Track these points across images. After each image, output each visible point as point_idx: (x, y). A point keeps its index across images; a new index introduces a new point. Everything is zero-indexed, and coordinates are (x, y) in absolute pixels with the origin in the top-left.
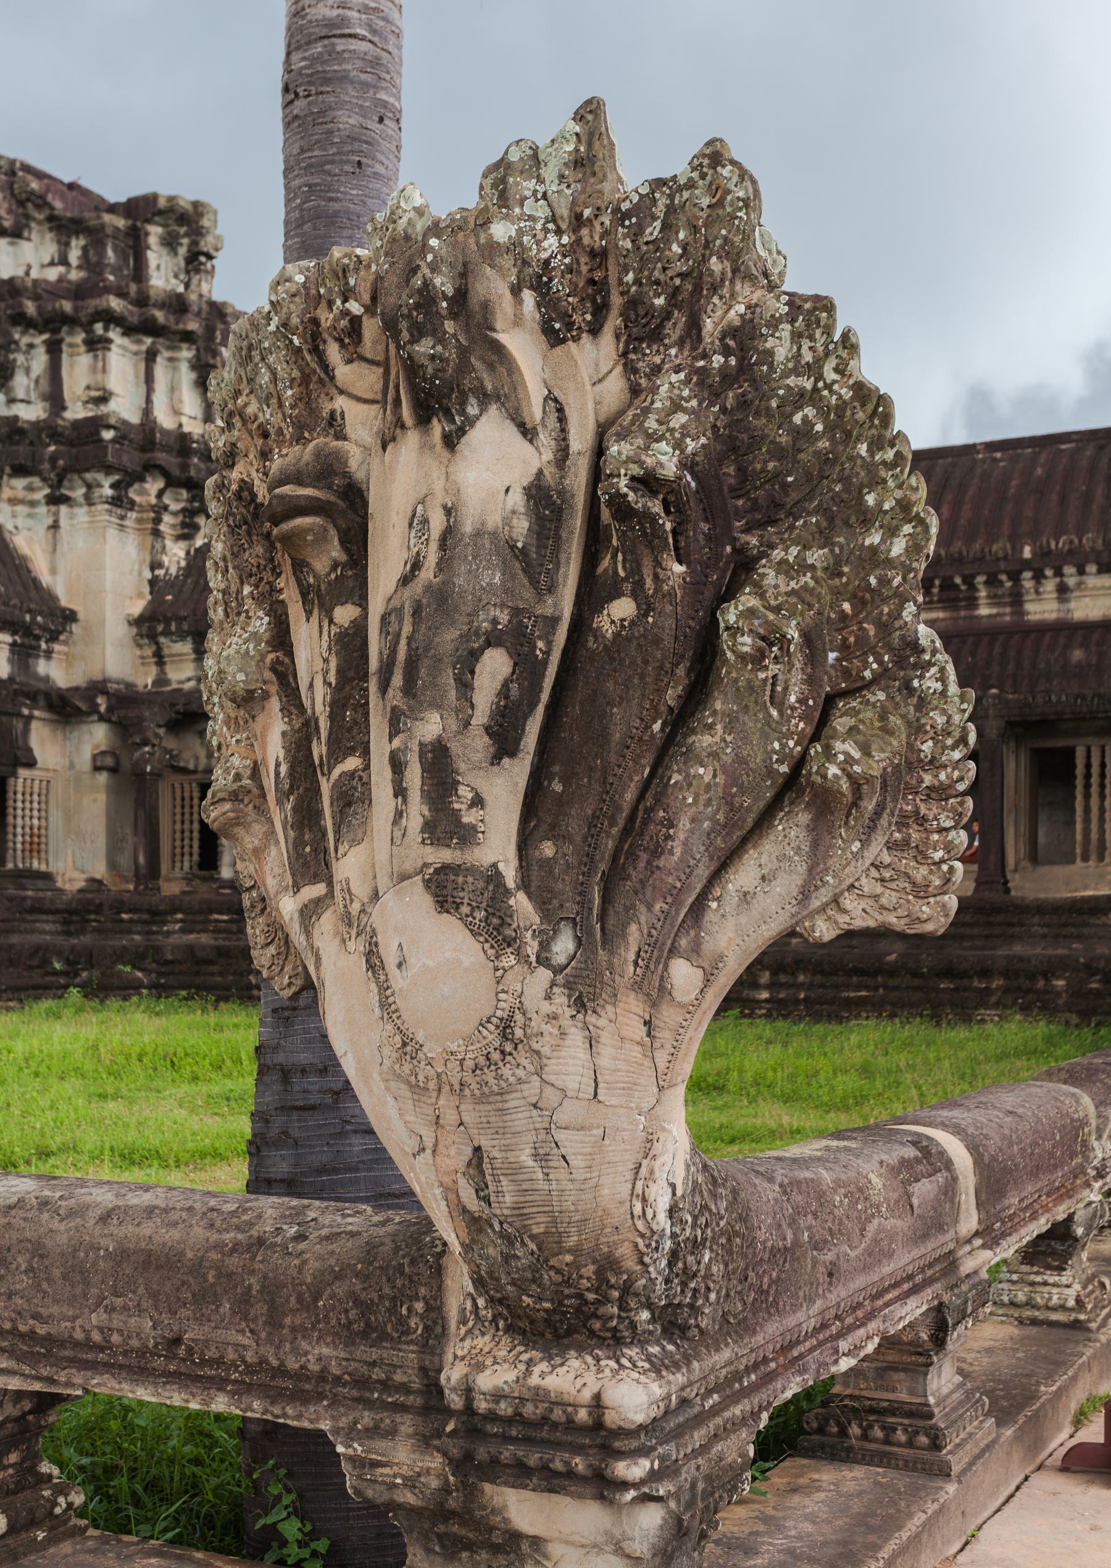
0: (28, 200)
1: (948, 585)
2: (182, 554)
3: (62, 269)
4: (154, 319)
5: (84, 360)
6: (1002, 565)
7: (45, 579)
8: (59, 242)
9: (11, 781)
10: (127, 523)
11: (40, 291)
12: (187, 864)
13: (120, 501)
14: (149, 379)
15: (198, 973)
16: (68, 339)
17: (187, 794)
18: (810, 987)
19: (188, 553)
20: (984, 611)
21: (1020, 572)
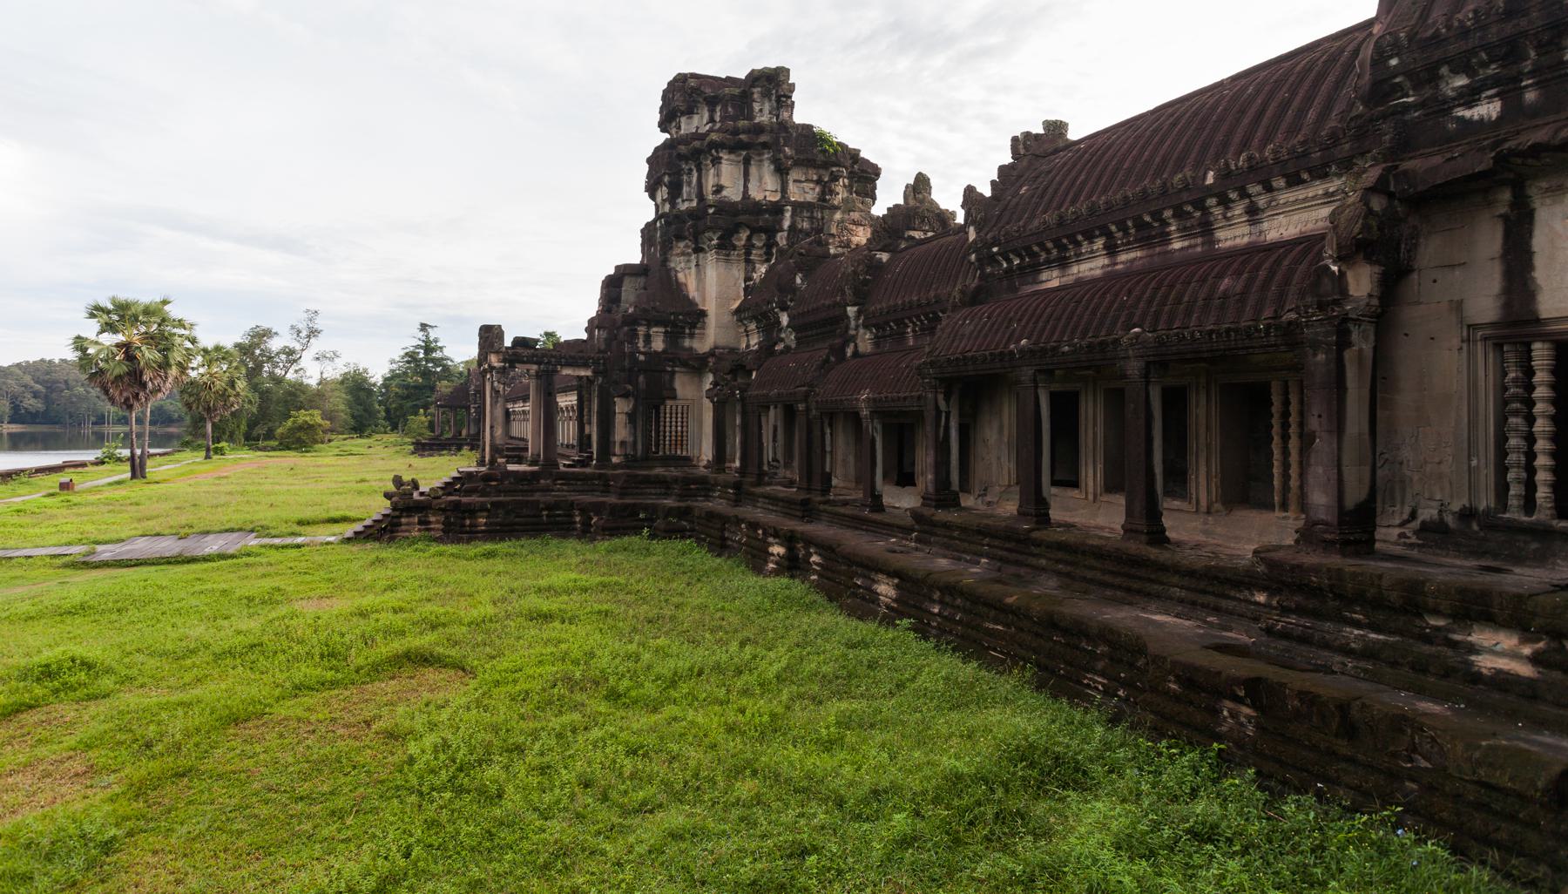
1: (1141, 225)
18: (964, 611)
21: (1203, 200)
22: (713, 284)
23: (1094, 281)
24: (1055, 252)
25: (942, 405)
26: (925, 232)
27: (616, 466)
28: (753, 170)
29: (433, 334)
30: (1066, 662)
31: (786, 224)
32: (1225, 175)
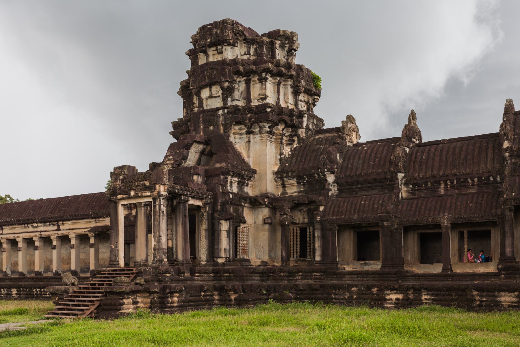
0: (238, 33)
2: (289, 150)
3: (248, 56)
4: (282, 71)
5: (258, 85)
7: (246, 159)
8: (247, 47)
11: (243, 63)
12: (295, 256)
13: (271, 133)
15: (312, 294)
16: (253, 79)
17: (295, 232)
19: (291, 149)
22: (263, 154)
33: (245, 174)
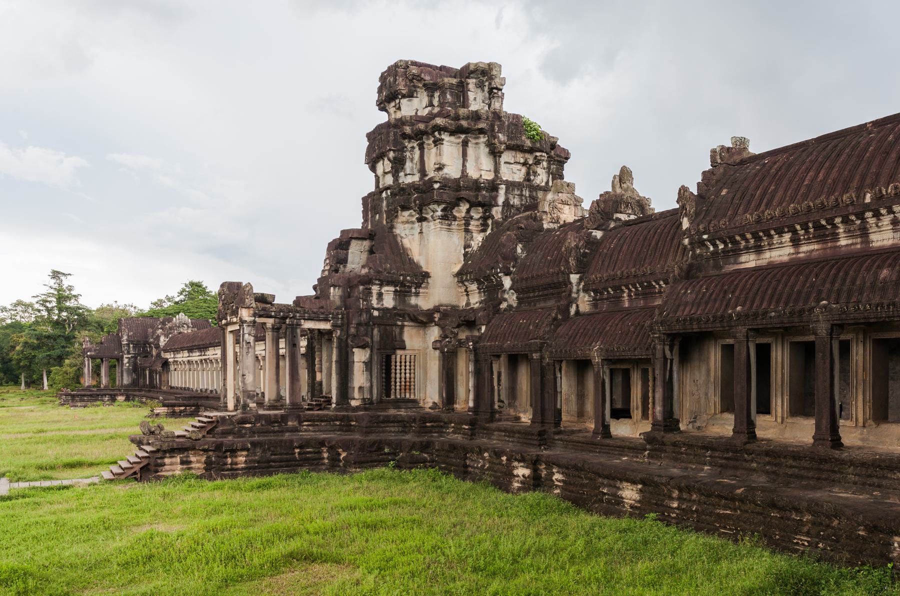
1: (818, 227)
3: (430, 108)
5: (434, 150)
6: (851, 209)
9: (393, 357)
10: (453, 227)
14: (464, 155)
18: (699, 503)
20: (843, 242)
21: (863, 213)
22: (438, 249)
23: (782, 266)
24: (752, 241)
25: (668, 353)
26: (629, 215)
27: (357, 409)
28: (470, 151)
29: (66, 282)
30: (780, 530)
31: (501, 200)
32: (879, 198)
33: (414, 278)
